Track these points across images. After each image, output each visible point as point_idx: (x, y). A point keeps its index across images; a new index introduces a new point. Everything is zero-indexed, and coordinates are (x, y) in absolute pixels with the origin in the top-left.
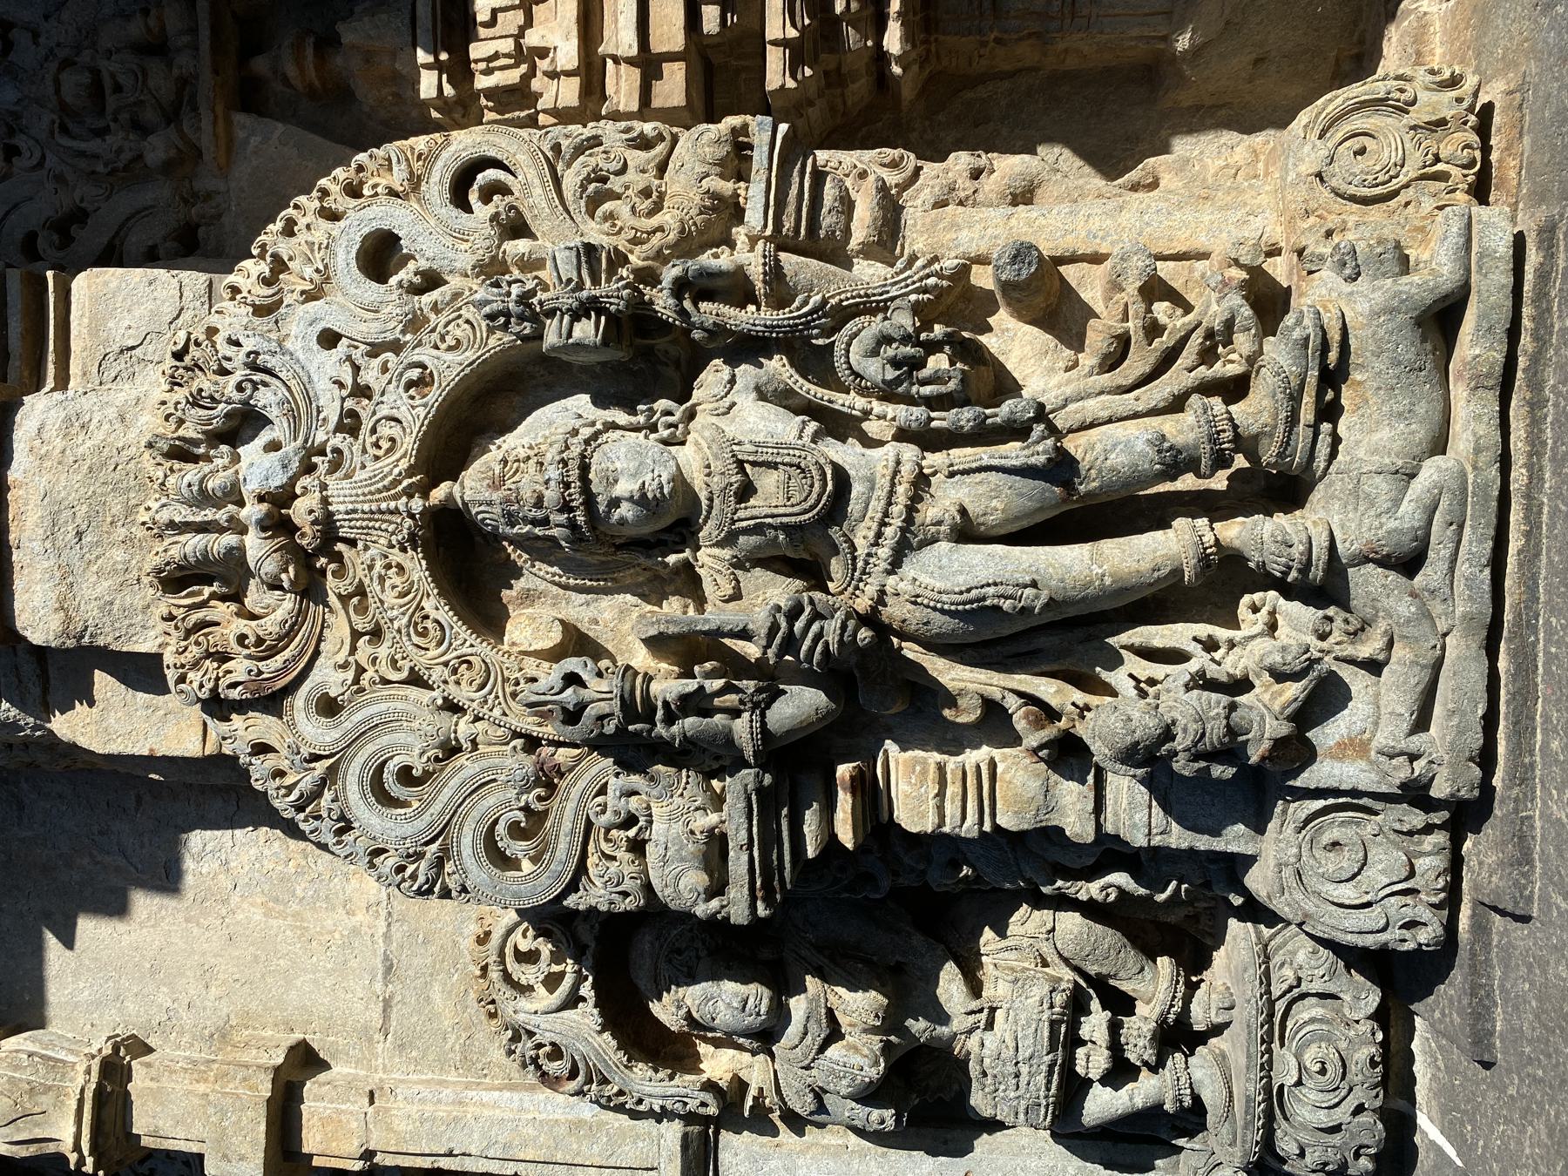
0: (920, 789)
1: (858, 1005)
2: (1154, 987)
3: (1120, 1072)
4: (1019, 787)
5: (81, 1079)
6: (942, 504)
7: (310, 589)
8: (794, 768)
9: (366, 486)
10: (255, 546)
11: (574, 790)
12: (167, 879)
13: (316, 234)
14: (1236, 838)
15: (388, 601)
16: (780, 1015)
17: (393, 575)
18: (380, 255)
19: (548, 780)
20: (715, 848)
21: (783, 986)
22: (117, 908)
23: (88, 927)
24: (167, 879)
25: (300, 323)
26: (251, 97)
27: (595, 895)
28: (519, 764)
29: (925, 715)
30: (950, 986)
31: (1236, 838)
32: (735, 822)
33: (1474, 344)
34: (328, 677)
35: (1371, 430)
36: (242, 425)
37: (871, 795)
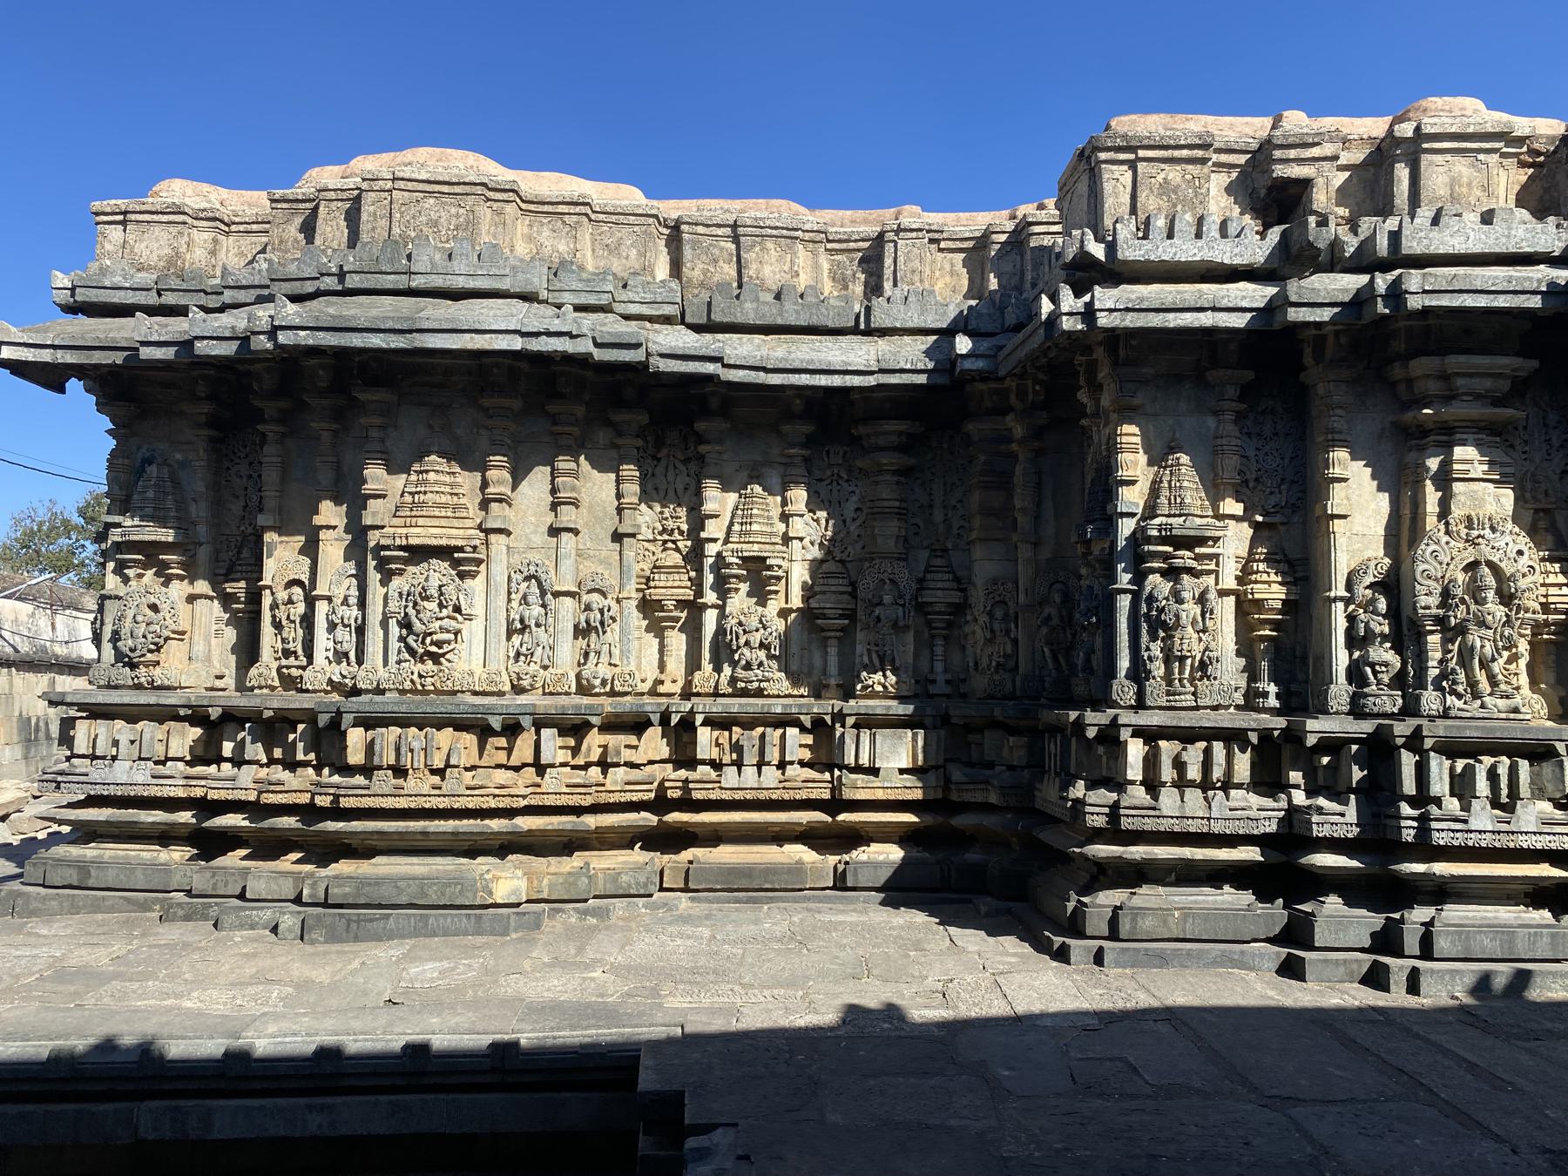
0: (1434, 640)
1: (1386, 630)
2: (1386, 678)
3: (1375, 673)
4: (1435, 655)
5: (1346, 474)
6: (1487, 644)
7: (1467, 541)
8: (1441, 621)
9: (1487, 552)
10: (1476, 533)
11: (1433, 584)
12: (1380, 489)
13: (1523, 542)
14: (1430, 687)
15: (1466, 554)
16: (1379, 615)
17: (1469, 555)
18: (1520, 553)
19: (1436, 580)
20: (1427, 607)
21: (1384, 616)
22: (1374, 477)
23: (1369, 470)
24: (1380, 489)
25: (1508, 538)
26: (1536, 511)
27: (1418, 587)
28: (1439, 575)
29: (1446, 641)
30: (1388, 645)
31: (1430, 687)
32: (1434, 611)
33: (1512, 716)
34: (1453, 543)
35: (1502, 703)
36: (1493, 529)
37: (1432, 632)
